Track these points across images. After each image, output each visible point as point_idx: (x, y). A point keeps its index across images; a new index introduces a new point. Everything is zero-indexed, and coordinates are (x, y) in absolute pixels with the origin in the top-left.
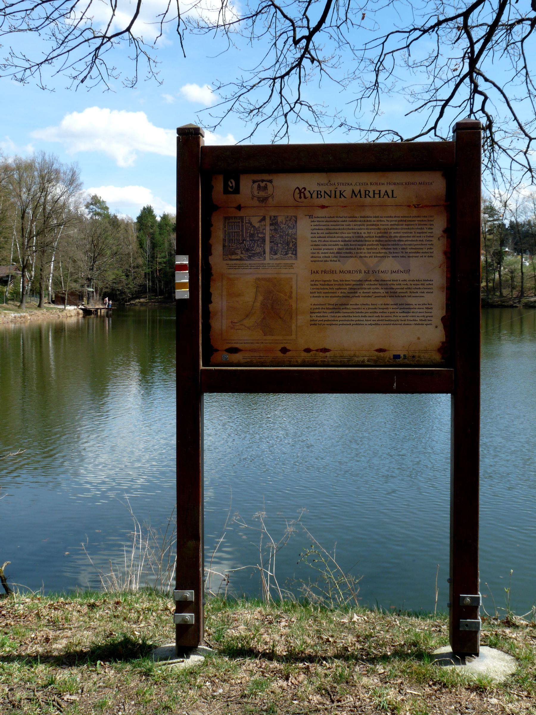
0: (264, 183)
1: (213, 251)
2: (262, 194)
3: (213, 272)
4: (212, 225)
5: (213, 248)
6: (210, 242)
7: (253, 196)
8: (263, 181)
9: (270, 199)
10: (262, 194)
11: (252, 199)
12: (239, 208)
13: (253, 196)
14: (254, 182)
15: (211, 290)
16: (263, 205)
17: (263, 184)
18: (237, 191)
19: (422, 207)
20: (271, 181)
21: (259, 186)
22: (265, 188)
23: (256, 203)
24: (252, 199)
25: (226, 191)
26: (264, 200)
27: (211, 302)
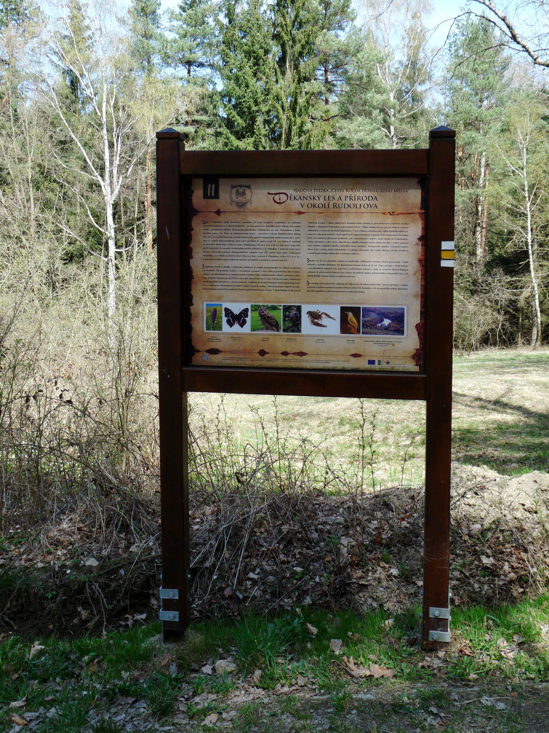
0: (243, 188)
1: (194, 255)
2: (241, 199)
3: (194, 274)
4: (192, 229)
5: (193, 251)
6: (192, 245)
7: (232, 201)
8: (241, 186)
9: (248, 205)
10: (241, 199)
11: (231, 204)
12: (218, 212)
13: (232, 201)
14: (233, 187)
15: (192, 293)
16: (242, 210)
17: (241, 190)
18: (217, 196)
19: (397, 215)
20: (249, 187)
21: (237, 191)
22: (244, 193)
23: (234, 208)
24: (231, 204)
25: (205, 196)
26: (242, 205)
27: (192, 304)
